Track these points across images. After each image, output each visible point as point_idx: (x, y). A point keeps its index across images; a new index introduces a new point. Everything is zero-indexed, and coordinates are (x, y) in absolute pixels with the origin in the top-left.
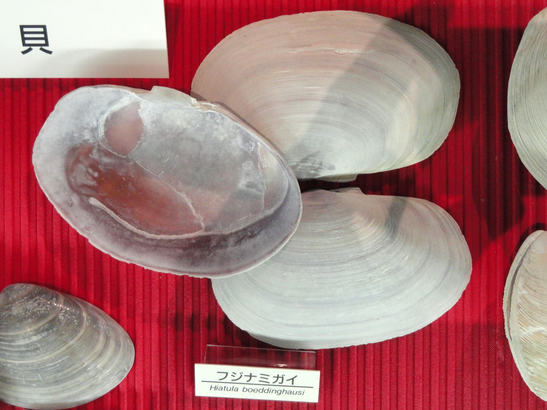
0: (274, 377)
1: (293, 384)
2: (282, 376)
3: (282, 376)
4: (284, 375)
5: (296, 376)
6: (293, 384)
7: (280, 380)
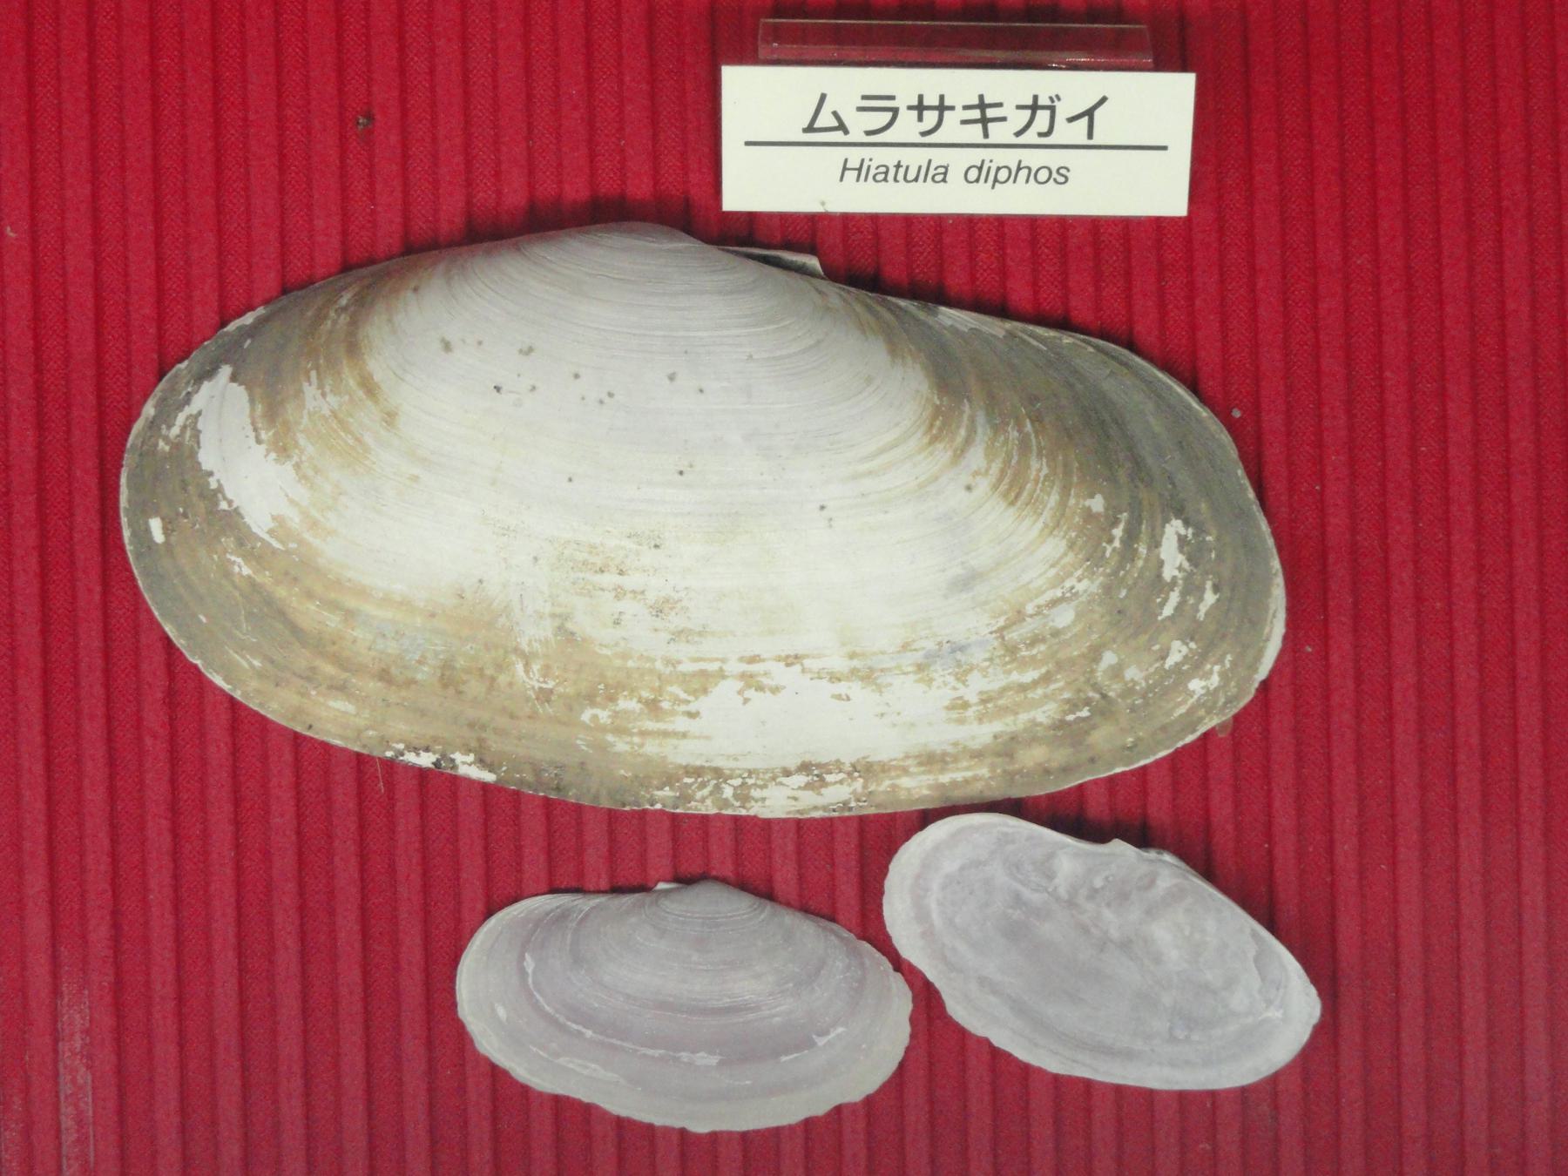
0: (1019, 107)
1: (1090, 136)
2: (1051, 99)
3: (1048, 103)
4: (1059, 99)
5: (1104, 100)
6: (1090, 136)
7: (1043, 118)
